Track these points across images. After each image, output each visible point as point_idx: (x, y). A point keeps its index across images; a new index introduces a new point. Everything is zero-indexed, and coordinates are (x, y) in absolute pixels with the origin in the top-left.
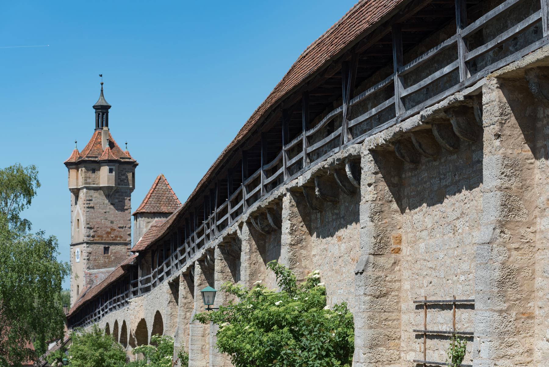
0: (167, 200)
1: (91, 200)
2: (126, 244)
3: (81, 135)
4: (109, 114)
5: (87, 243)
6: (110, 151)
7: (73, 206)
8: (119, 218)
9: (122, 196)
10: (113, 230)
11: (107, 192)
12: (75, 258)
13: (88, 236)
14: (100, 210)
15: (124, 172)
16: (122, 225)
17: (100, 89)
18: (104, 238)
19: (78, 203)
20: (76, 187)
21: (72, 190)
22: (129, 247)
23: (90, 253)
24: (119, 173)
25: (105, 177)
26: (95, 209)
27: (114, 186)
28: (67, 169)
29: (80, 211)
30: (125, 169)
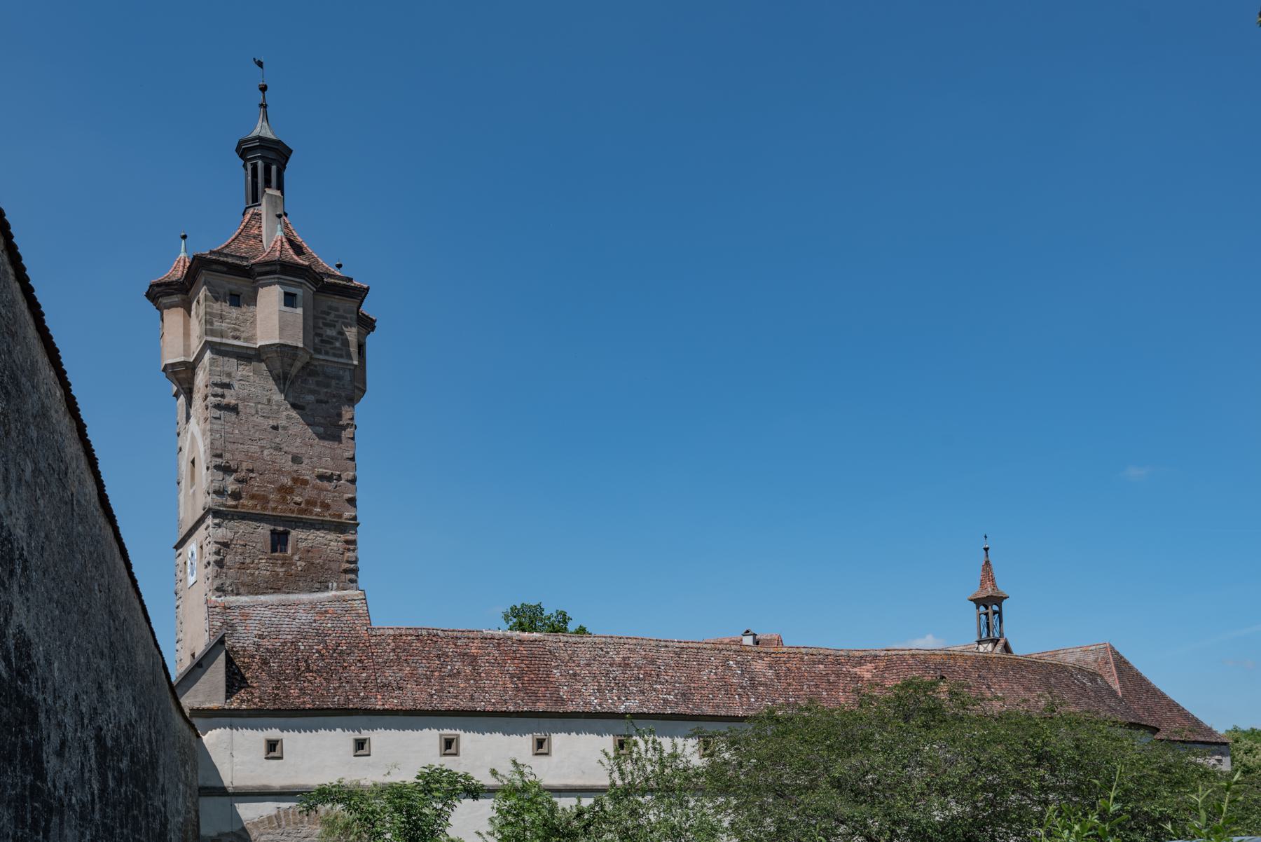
1: (228, 386)
5: (216, 514)
6: (286, 245)
11: (278, 364)
13: (220, 493)
14: (259, 420)
18: (272, 504)
20: (182, 359)
23: (226, 545)
25: (271, 318)
27: (301, 345)
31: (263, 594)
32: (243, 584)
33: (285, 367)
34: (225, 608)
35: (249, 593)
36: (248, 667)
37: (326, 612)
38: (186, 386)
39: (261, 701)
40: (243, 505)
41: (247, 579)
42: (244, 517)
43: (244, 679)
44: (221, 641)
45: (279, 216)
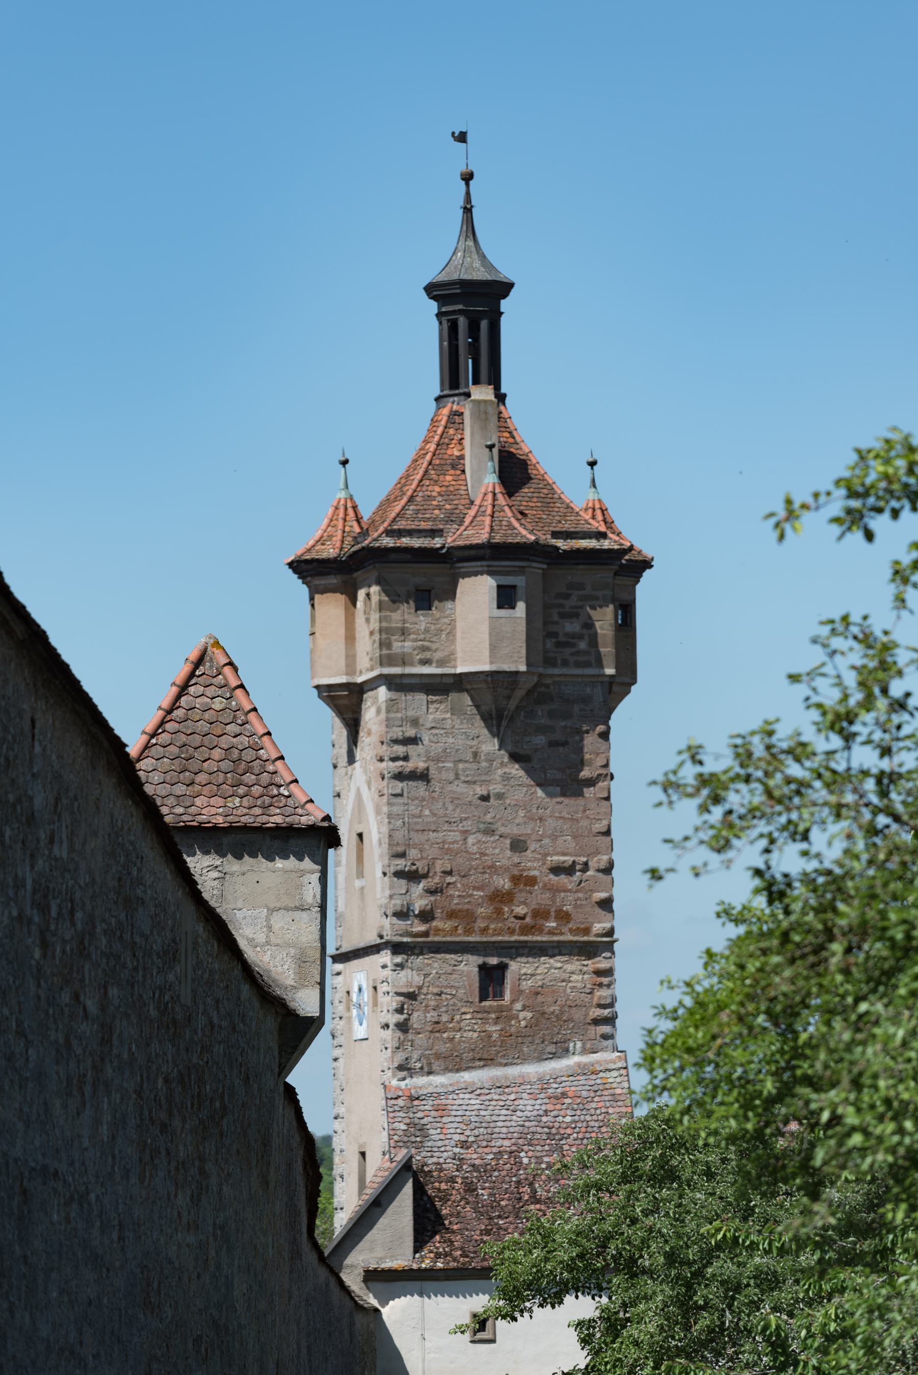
0: (226, 765)
2: (589, 950)
3: (369, 427)
4: (504, 322)
5: (397, 948)
6: (502, 500)
7: (341, 771)
8: (551, 823)
9: (567, 716)
10: (523, 881)
12: (350, 1019)
13: (402, 914)
14: (460, 788)
15: (573, 601)
16: (569, 859)
17: (461, 202)
19: (358, 754)
20: (343, 679)
21: (328, 693)
22: (603, 965)
23: (412, 996)
24: (547, 607)
25: (477, 628)
26: (436, 785)
27: (523, 668)
28: (304, 590)
29: (366, 794)
30: (581, 586)
31: (468, 1069)
32: (438, 1056)
33: (500, 702)
34: (412, 1098)
35: (447, 1070)
36: (445, 1199)
37: (564, 1095)
38: (349, 715)
39: (464, 1255)
40: (438, 931)
41: (443, 1048)
42: (438, 948)
43: (439, 1218)
44: (407, 1167)
45: (491, 447)
